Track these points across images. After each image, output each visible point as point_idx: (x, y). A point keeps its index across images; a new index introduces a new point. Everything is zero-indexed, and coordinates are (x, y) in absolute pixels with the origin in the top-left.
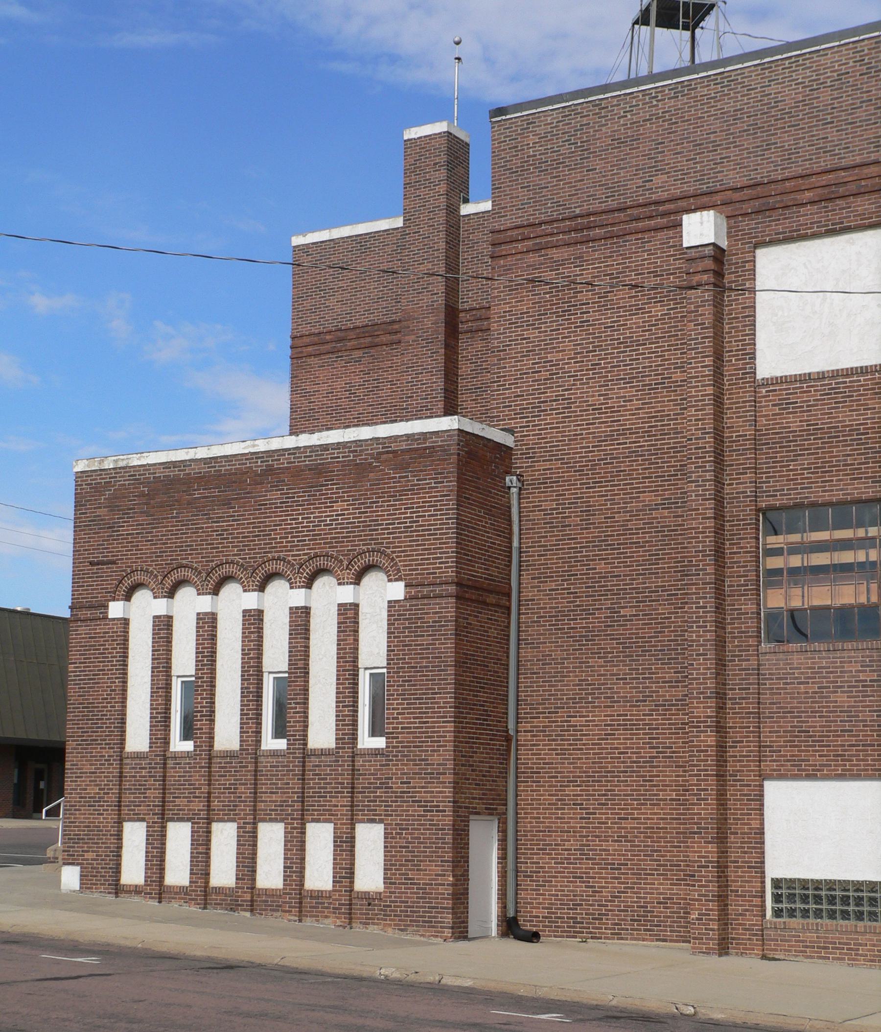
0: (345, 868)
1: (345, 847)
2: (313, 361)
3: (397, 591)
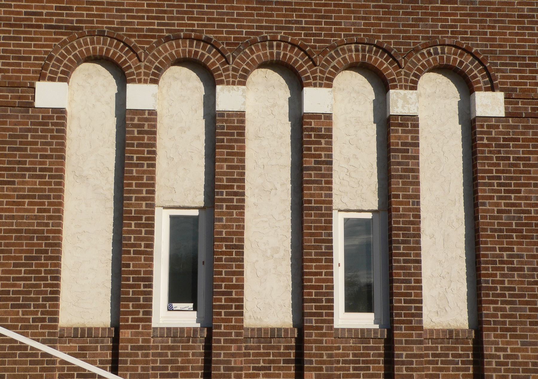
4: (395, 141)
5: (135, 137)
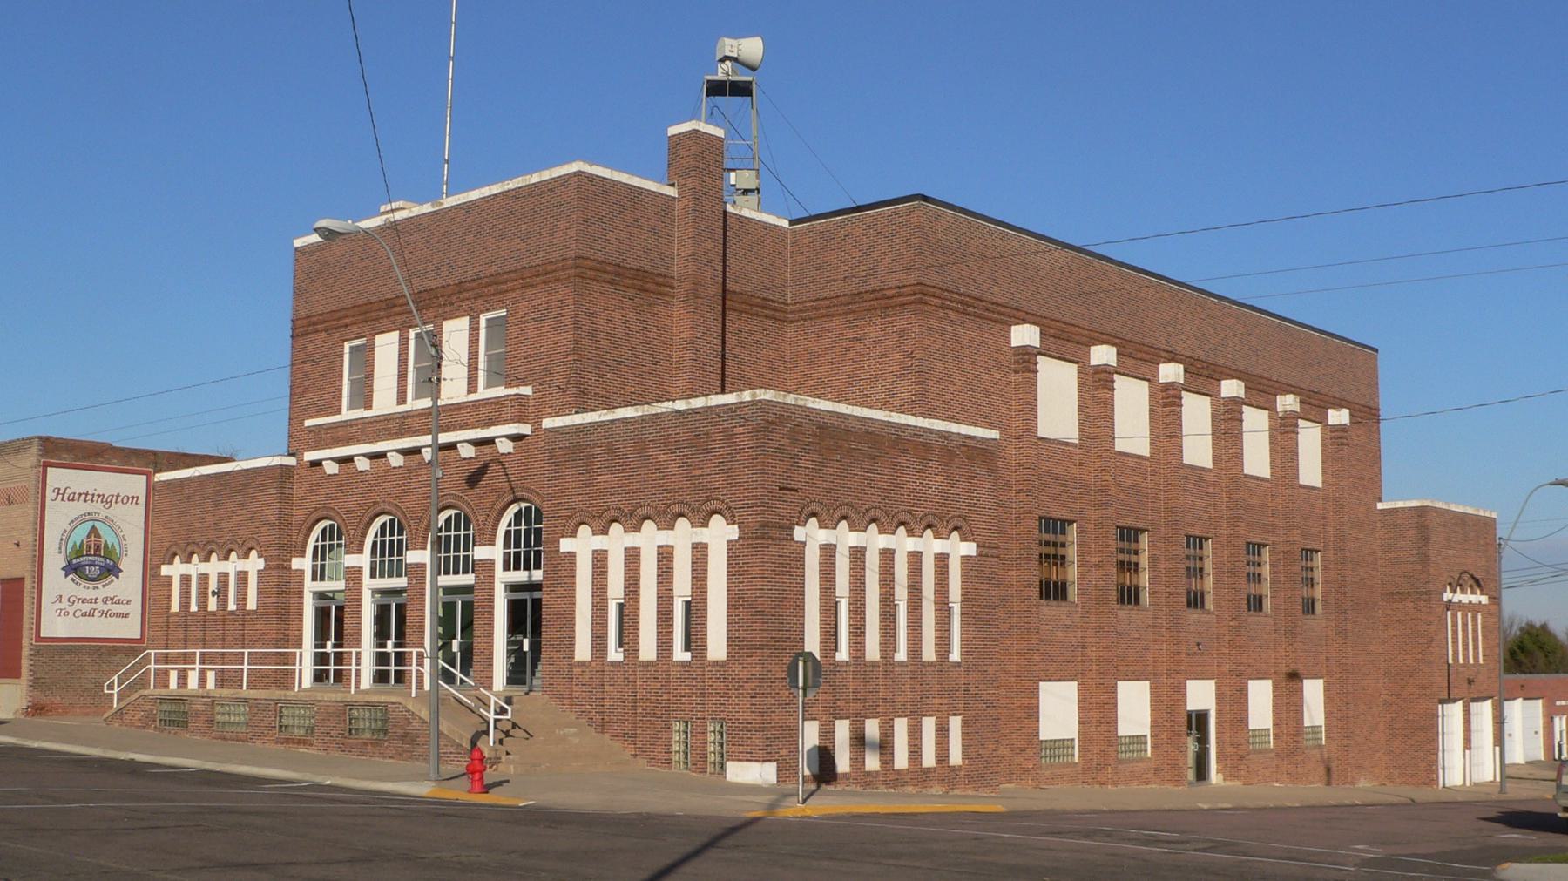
0: (915, 751)
1: (942, 732)
2: (597, 286)
3: (969, 548)
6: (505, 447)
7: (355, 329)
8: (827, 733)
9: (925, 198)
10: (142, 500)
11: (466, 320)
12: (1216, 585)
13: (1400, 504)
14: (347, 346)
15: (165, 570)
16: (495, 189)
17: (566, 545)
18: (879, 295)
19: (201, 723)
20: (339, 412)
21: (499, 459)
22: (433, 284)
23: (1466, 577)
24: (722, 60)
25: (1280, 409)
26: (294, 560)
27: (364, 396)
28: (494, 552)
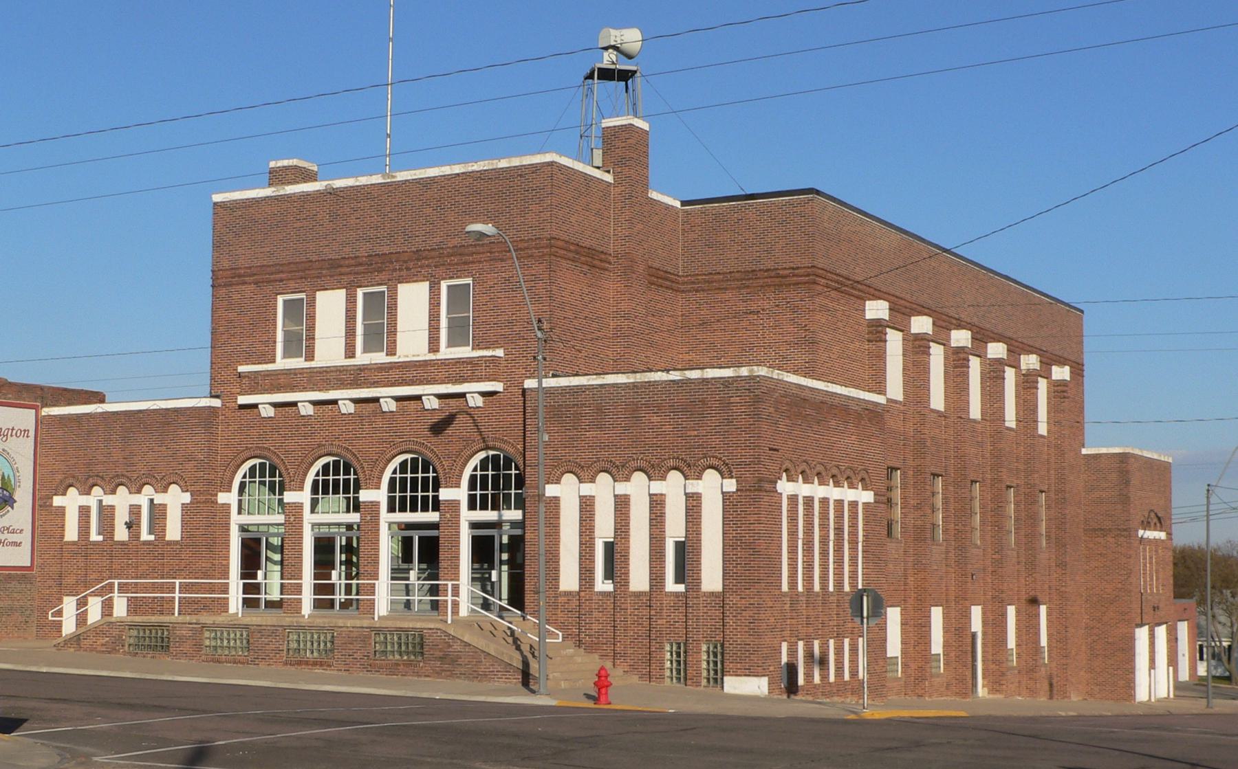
2: (564, 263)
4: (693, 504)
5: (587, 506)
6: (476, 401)
7: (292, 284)
8: (793, 652)
9: (818, 192)
10: (32, 433)
11: (425, 285)
12: (983, 523)
13: (1104, 450)
14: (280, 299)
15: (57, 501)
16: (457, 169)
17: (551, 490)
18: (773, 274)
19: (187, 647)
20: (274, 362)
21: (469, 412)
22: (386, 250)
23: (1152, 515)
24: (606, 49)
25: (1023, 367)
26: (220, 494)
27: (302, 342)
28: (457, 494)
